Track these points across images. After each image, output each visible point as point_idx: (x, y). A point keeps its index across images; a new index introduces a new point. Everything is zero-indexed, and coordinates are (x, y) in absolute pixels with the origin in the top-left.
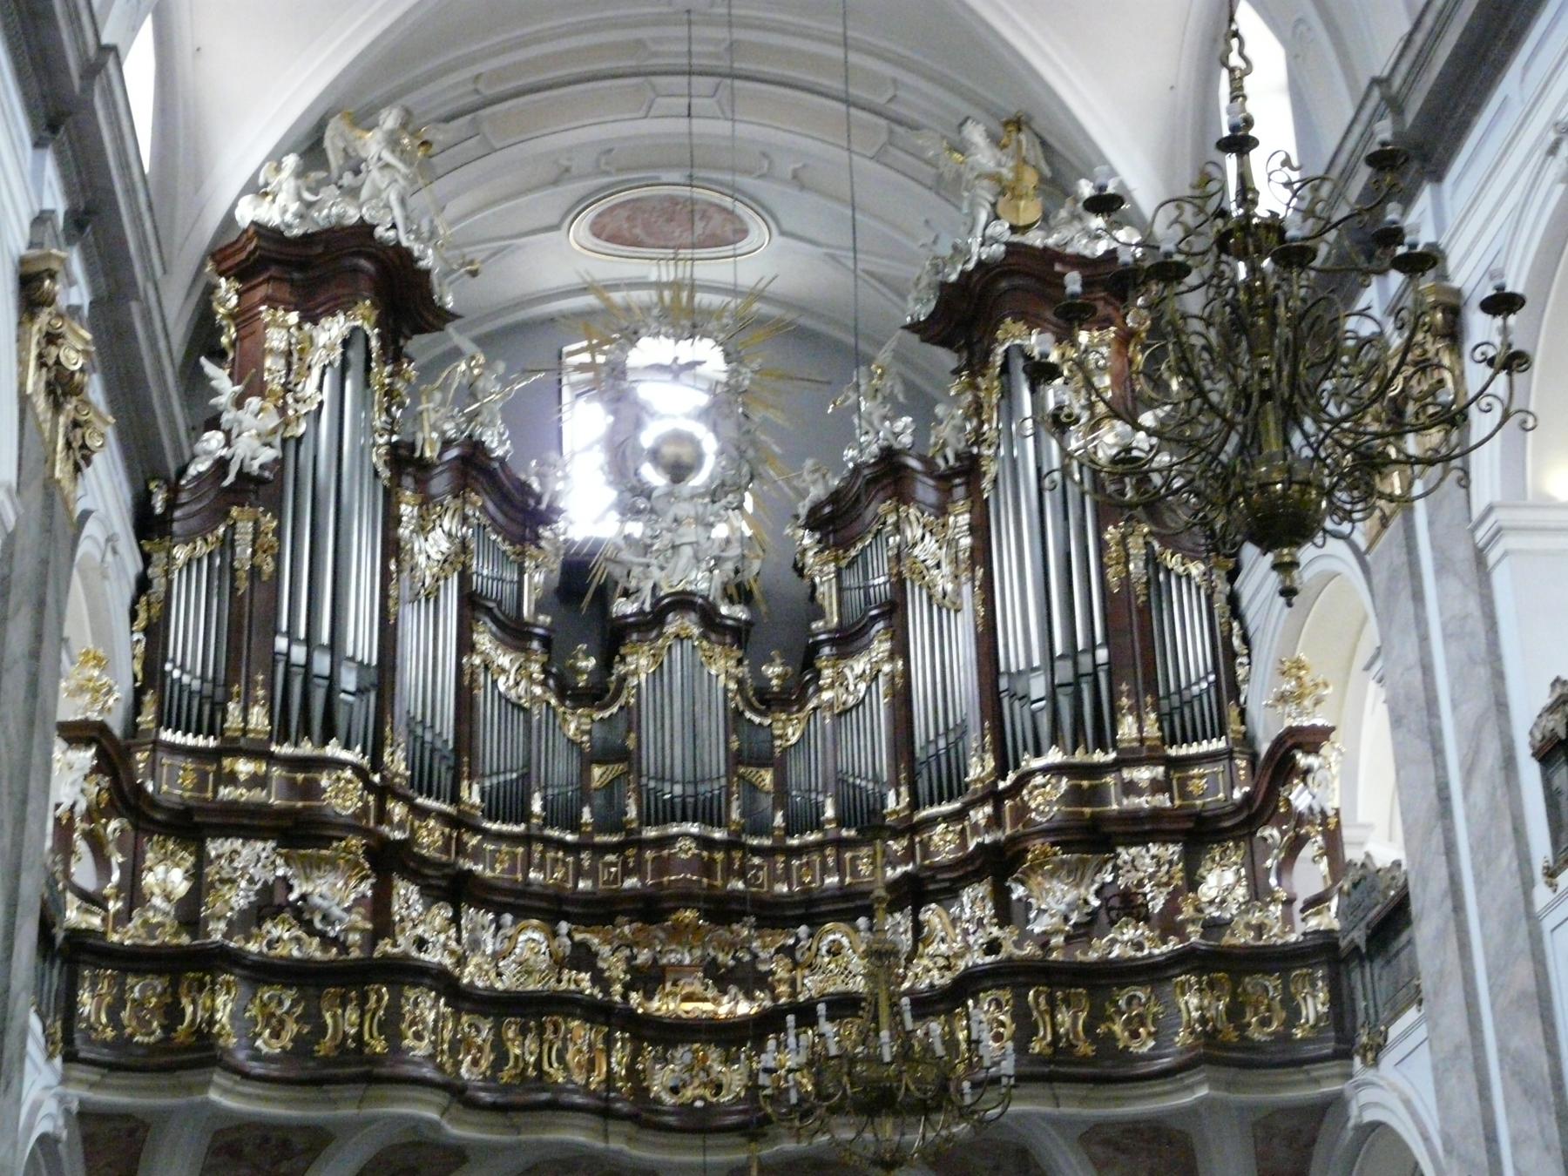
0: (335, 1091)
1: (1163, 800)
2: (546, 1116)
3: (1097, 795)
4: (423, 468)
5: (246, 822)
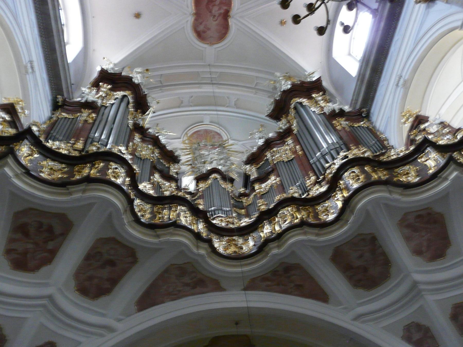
2: (171, 230)
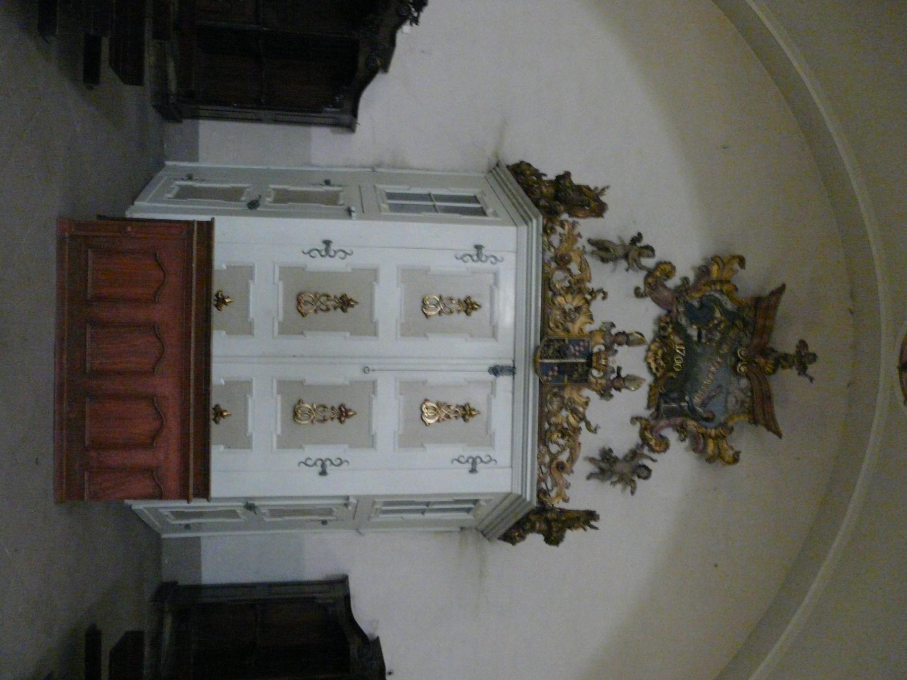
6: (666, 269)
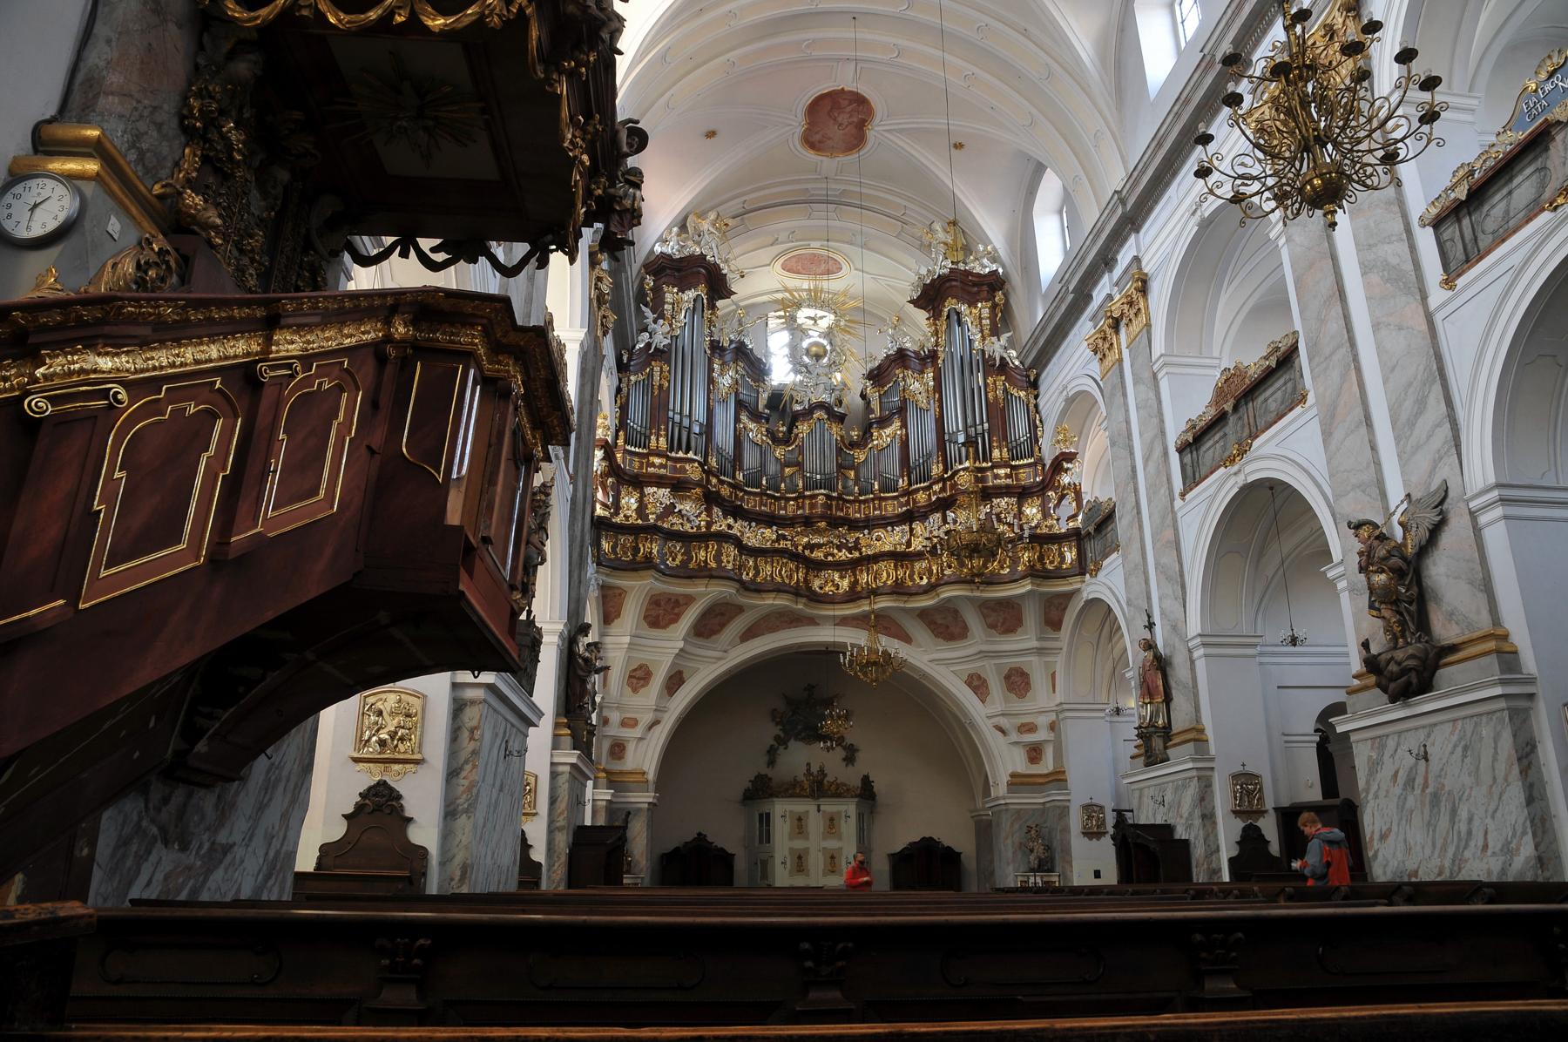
0: (697, 581)
1: (1009, 481)
3: (983, 480)
4: (723, 349)
5: (659, 482)
6: (777, 738)
